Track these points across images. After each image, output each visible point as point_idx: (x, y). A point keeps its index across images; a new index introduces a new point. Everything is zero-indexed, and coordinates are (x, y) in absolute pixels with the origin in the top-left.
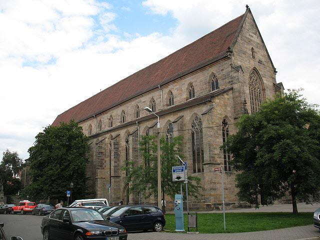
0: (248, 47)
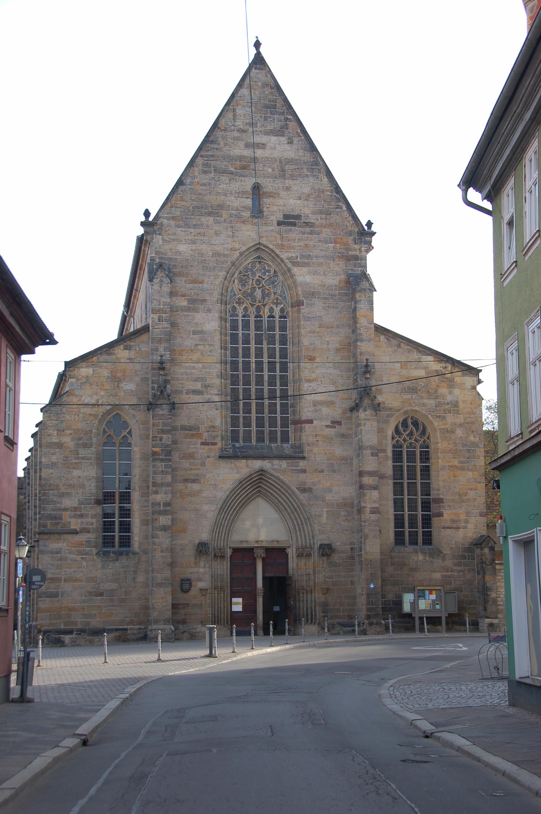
0: (235, 186)
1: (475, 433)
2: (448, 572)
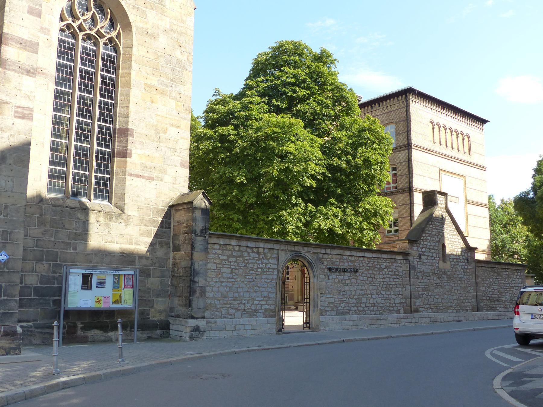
1: (183, 49)
2: (131, 243)
